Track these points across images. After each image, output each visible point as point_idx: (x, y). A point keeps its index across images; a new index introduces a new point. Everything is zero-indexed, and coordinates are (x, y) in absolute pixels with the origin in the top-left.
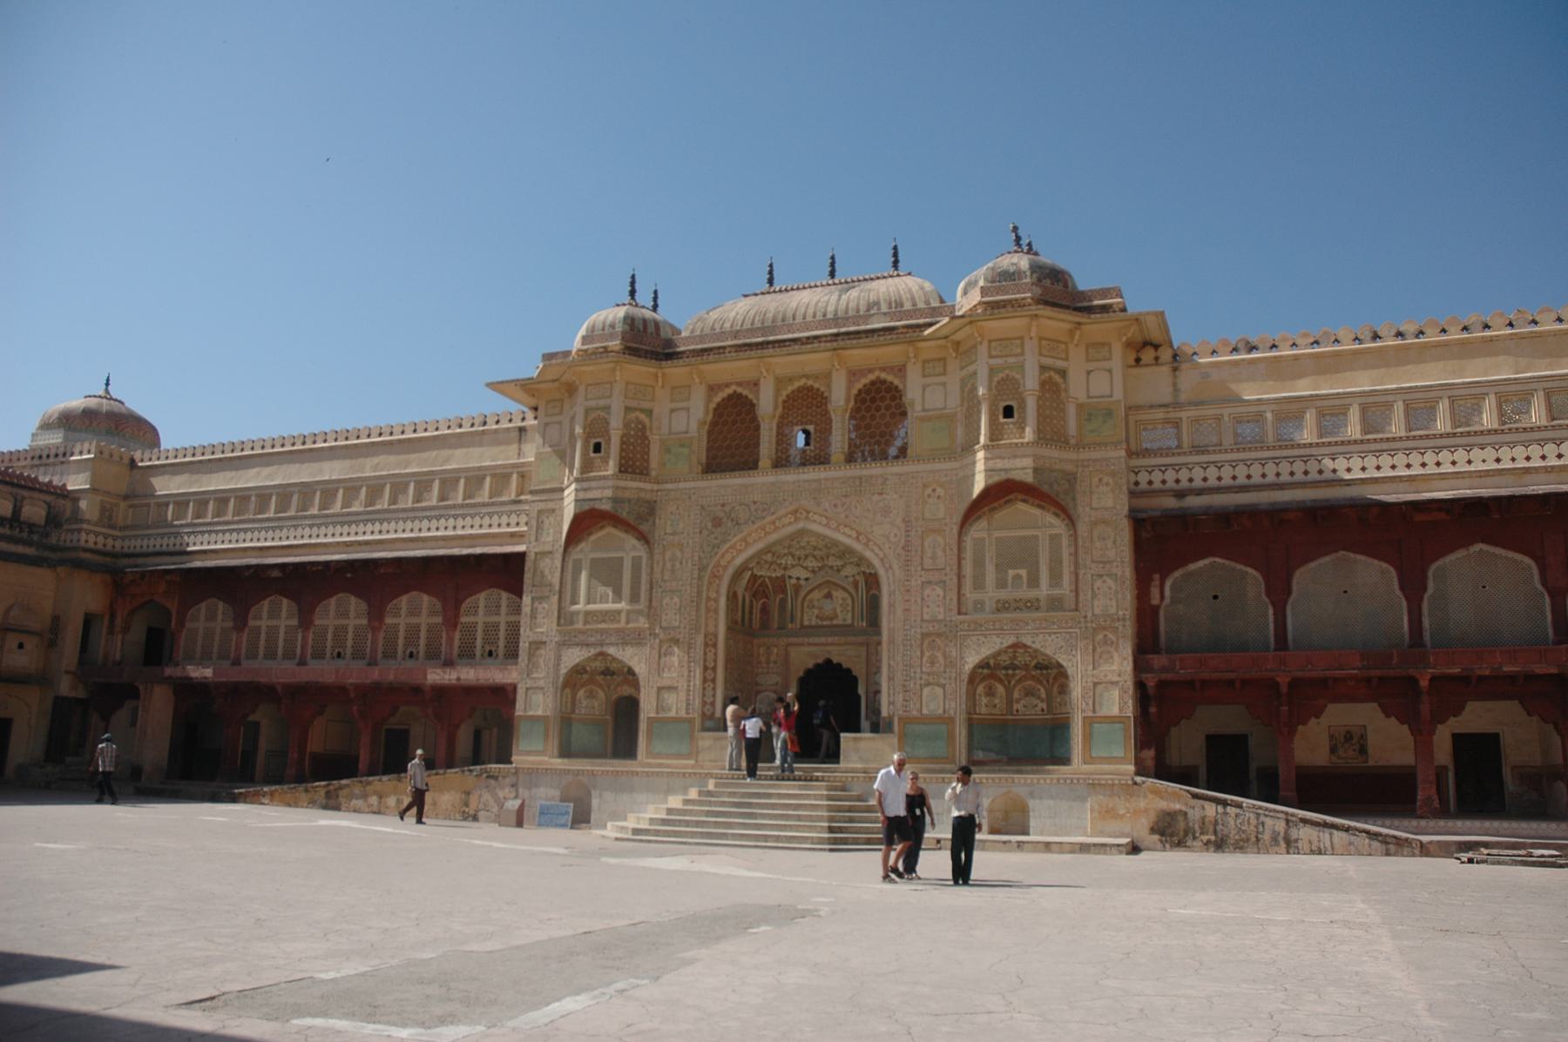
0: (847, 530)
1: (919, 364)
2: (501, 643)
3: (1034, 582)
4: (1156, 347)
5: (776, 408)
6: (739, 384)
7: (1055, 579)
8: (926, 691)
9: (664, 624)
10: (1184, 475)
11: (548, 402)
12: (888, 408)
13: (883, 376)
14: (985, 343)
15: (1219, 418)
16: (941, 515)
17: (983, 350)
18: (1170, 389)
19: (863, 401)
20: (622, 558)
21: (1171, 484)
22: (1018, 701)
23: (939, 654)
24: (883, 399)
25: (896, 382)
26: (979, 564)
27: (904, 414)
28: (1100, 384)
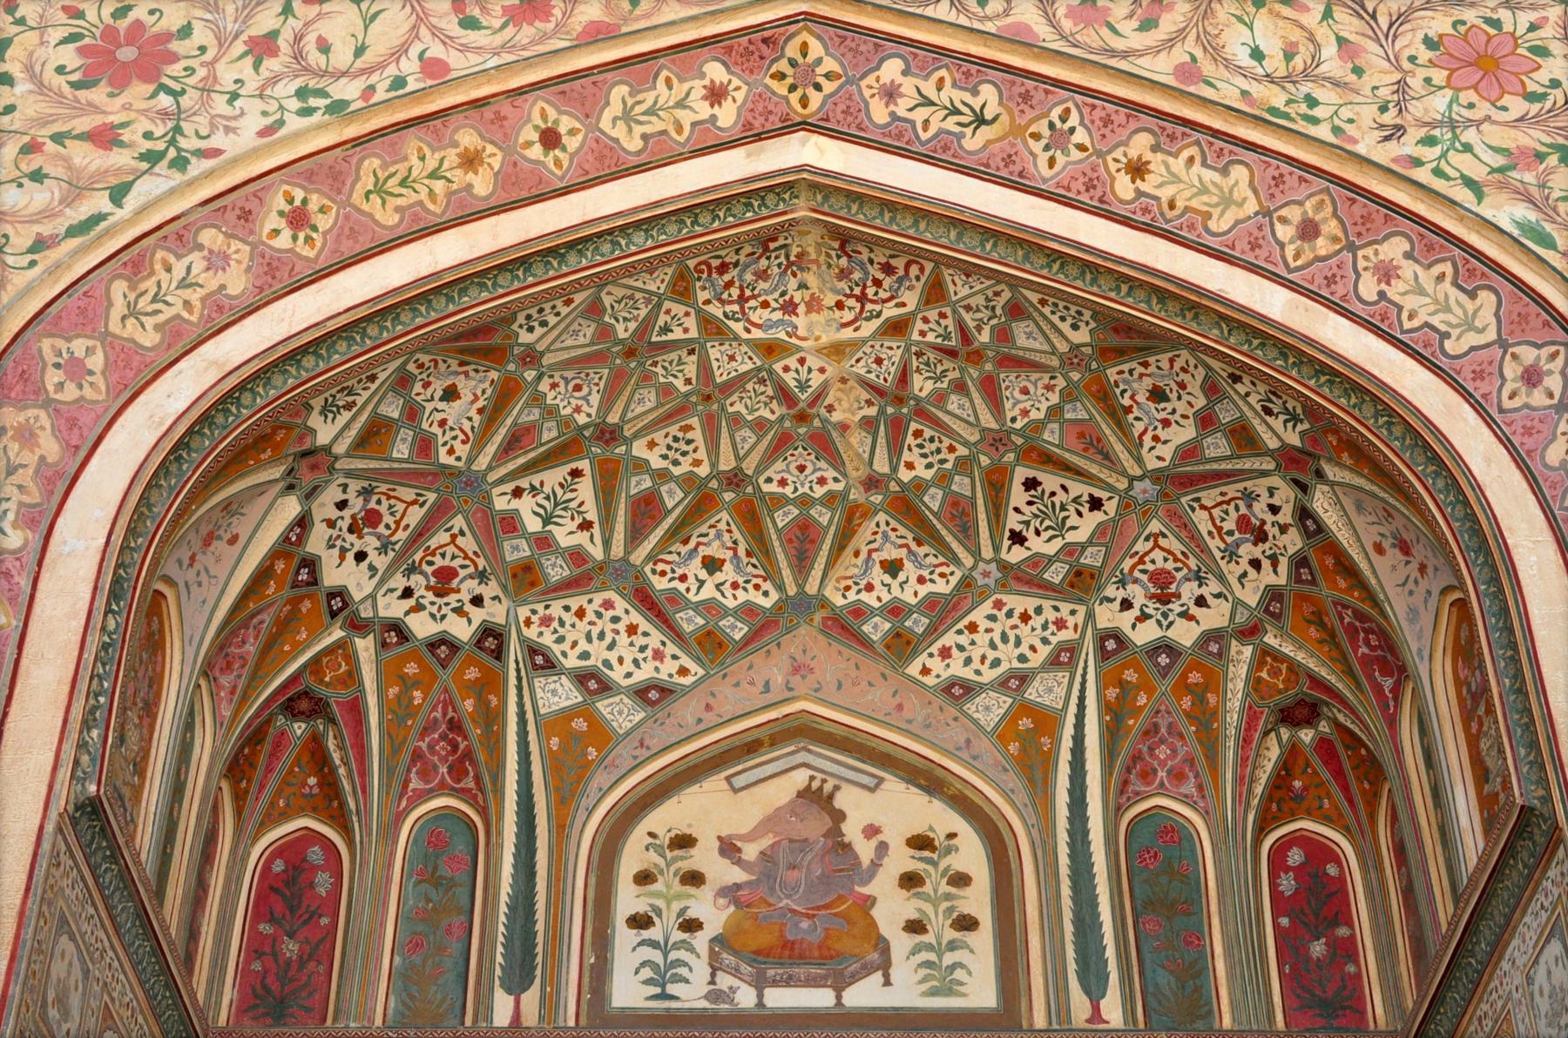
0: (1179, 178)
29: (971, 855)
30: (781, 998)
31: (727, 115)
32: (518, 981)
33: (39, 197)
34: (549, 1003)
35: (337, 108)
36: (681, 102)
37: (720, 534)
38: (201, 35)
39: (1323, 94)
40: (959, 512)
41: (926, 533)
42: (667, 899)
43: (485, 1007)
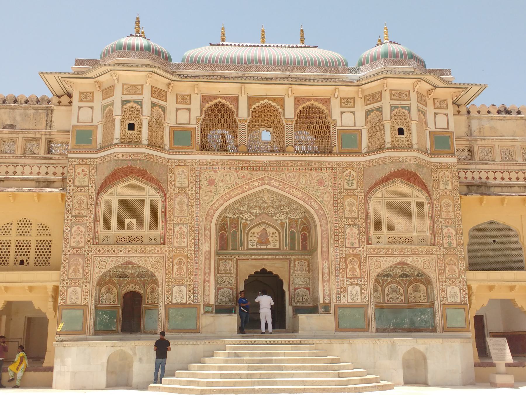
0: (296, 192)
1: (339, 99)
2: (32, 255)
3: (409, 228)
4: (459, 106)
5: (248, 116)
6: (224, 98)
7: (421, 228)
8: (350, 288)
9: (176, 244)
10: (476, 175)
11: (80, 92)
12: (318, 123)
13: (316, 103)
14: (388, 93)
15: (493, 147)
16: (355, 187)
17: (386, 96)
18: (467, 129)
19: (303, 117)
20: (143, 201)
21: (469, 179)
22: (388, 295)
23: (357, 267)
24: (315, 117)
25: (324, 108)
26: (377, 215)
27: (328, 127)
28: (442, 122)
29: (277, 234)
30: (262, 247)
31: (259, 184)
32: (241, 246)
33: (207, 198)
34: (244, 248)
35: (229, 188)
36: (256, 184)
37: (257, 208)
38: (217, 180)
39: (308, 186)
40: (278, 208)
41: (274, 208)
42: (253, 238)
43: (239, 248)
